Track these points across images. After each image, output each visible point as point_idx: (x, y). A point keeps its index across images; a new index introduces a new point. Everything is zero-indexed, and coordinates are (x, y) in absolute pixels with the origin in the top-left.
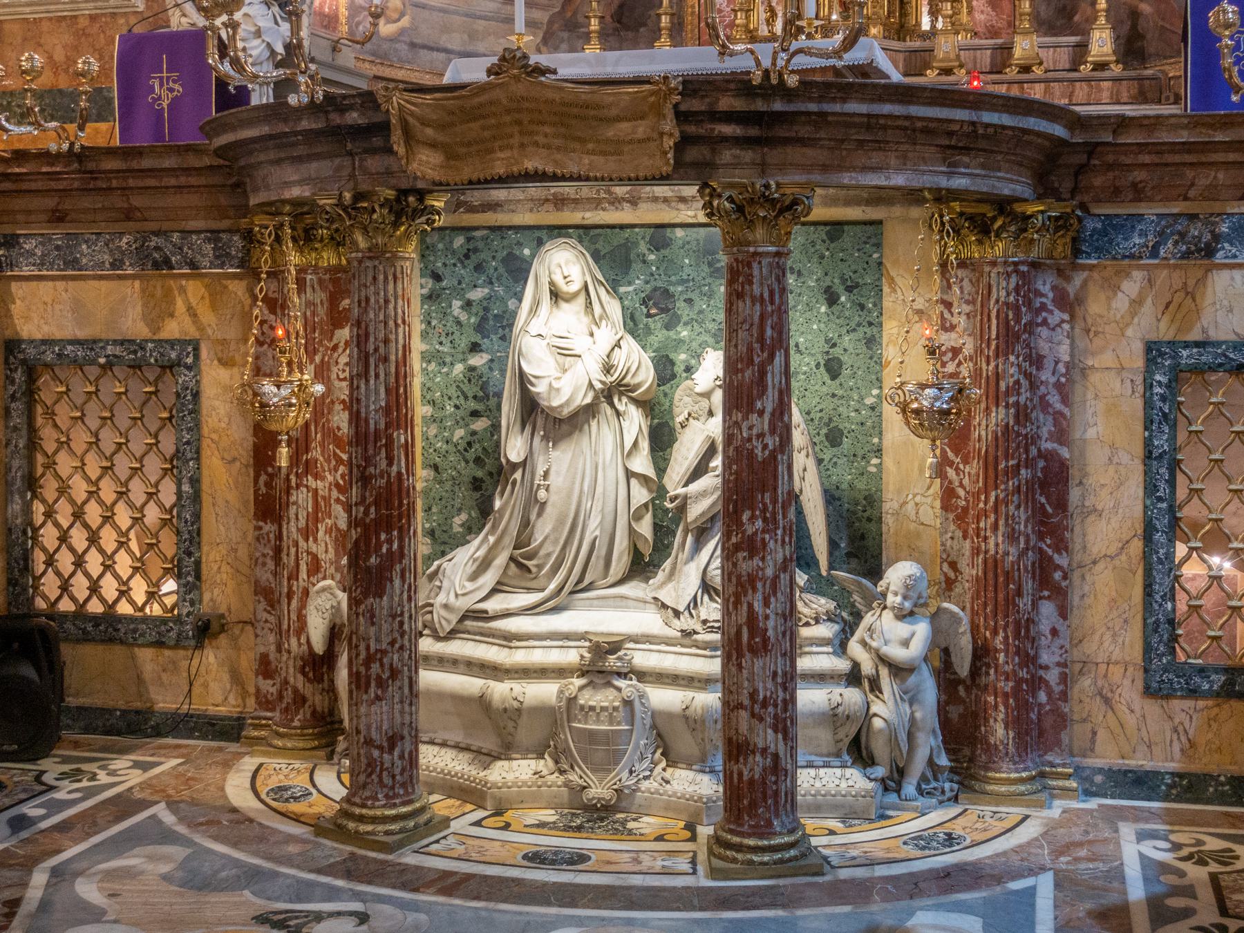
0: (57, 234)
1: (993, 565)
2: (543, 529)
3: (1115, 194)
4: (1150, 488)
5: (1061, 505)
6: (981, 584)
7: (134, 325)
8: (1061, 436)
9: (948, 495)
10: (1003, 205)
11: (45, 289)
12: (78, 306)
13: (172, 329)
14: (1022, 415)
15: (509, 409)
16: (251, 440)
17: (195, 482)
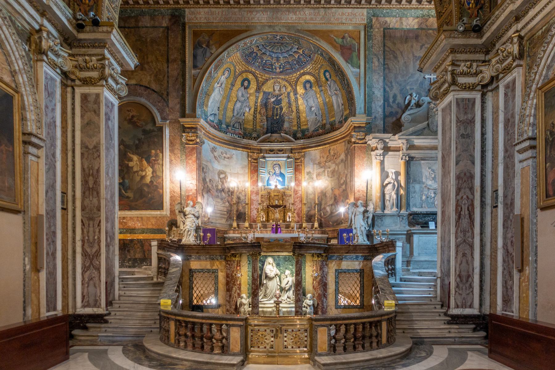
0: (197, 255)
1: (319, 294)
2: (268, 291)
3: (332, 253)
4: (336, 285)
5: (326, 287)
6: (318, 296)
7: (209, 267)
8: (326, 280)
9: (313, 287)
10: (320, 254)
11: (195, 262)
12: (200, 265)
13: (214, 268)
14: (322, 277)
15: (263, 277)
16: (225, 282)
17: (217, 287)
